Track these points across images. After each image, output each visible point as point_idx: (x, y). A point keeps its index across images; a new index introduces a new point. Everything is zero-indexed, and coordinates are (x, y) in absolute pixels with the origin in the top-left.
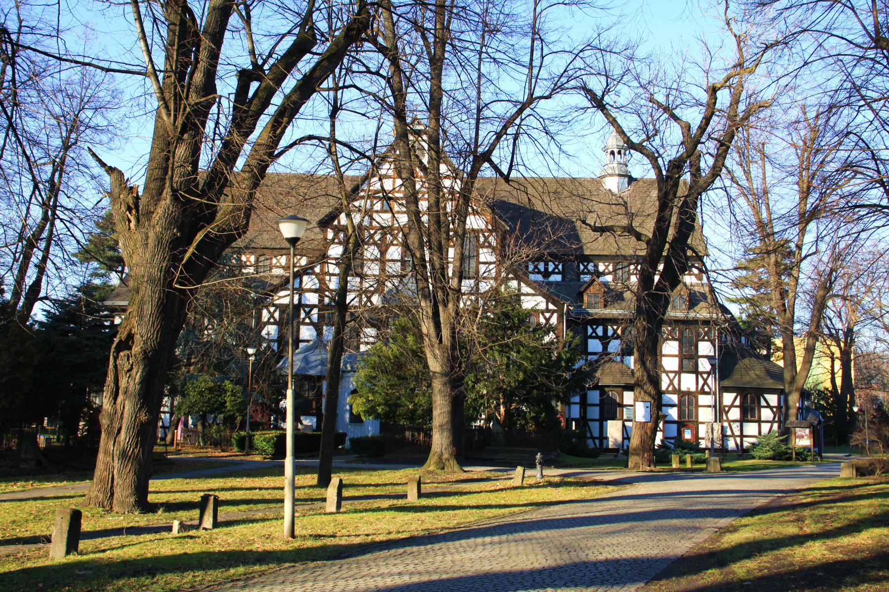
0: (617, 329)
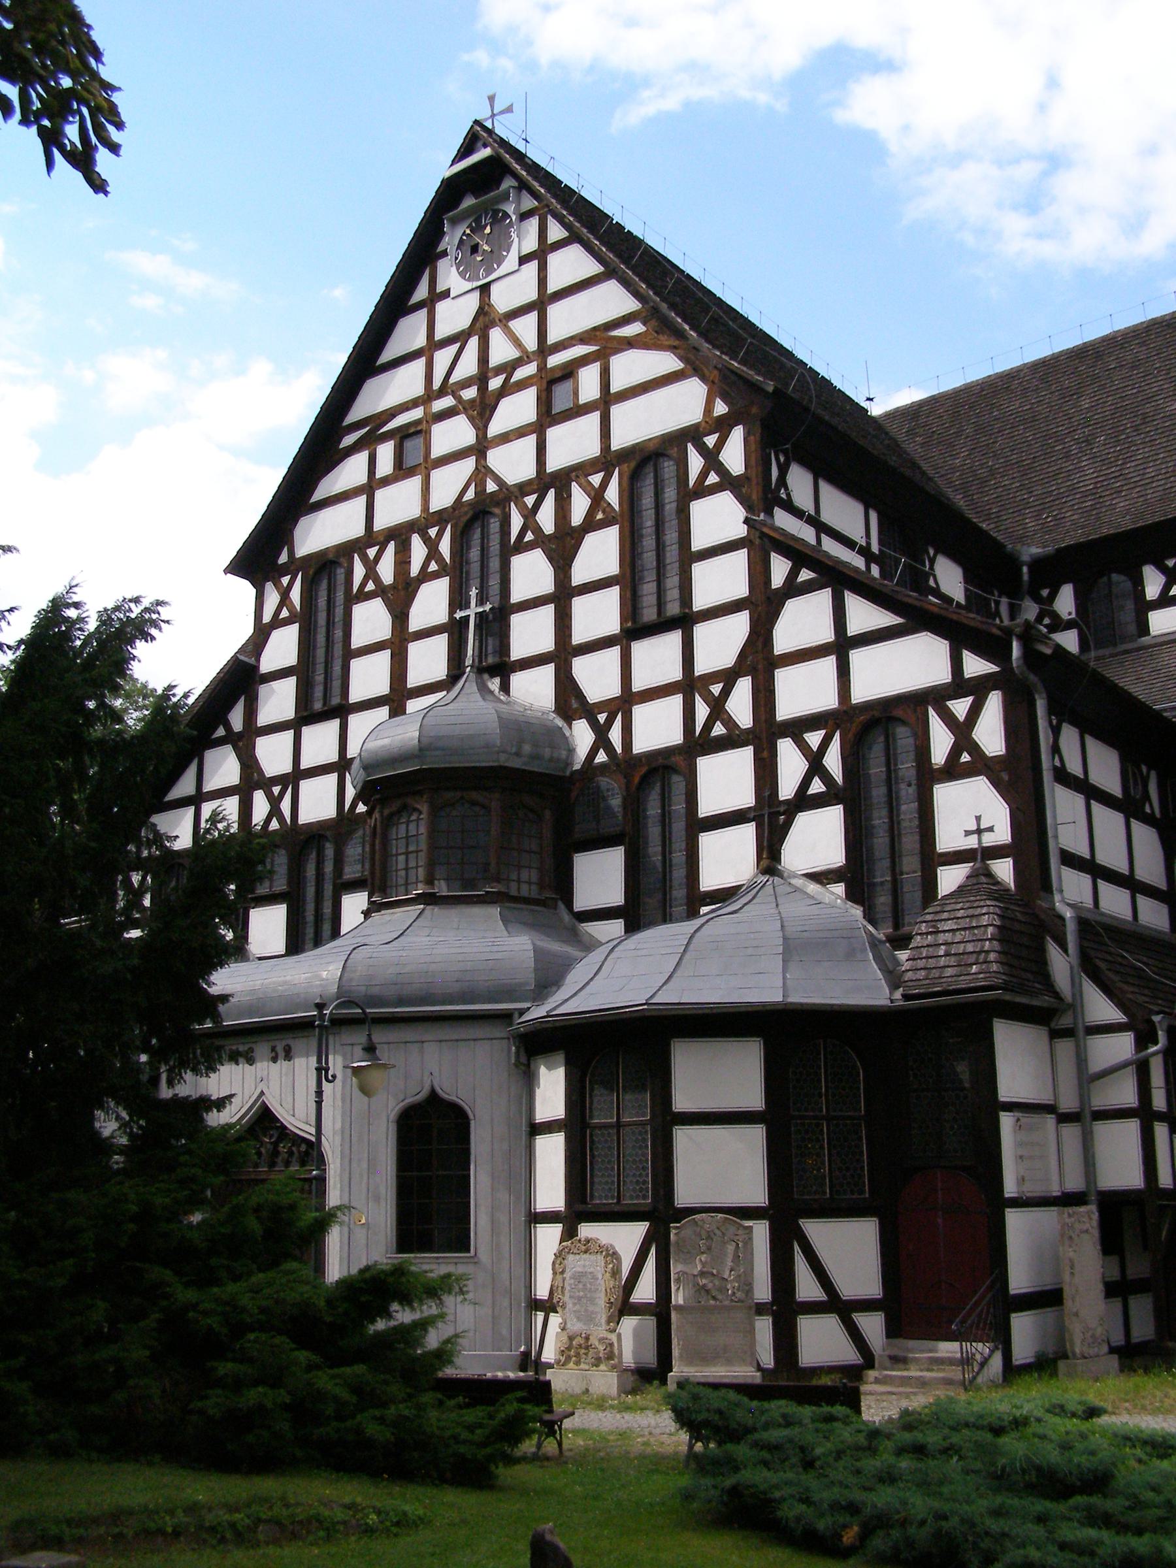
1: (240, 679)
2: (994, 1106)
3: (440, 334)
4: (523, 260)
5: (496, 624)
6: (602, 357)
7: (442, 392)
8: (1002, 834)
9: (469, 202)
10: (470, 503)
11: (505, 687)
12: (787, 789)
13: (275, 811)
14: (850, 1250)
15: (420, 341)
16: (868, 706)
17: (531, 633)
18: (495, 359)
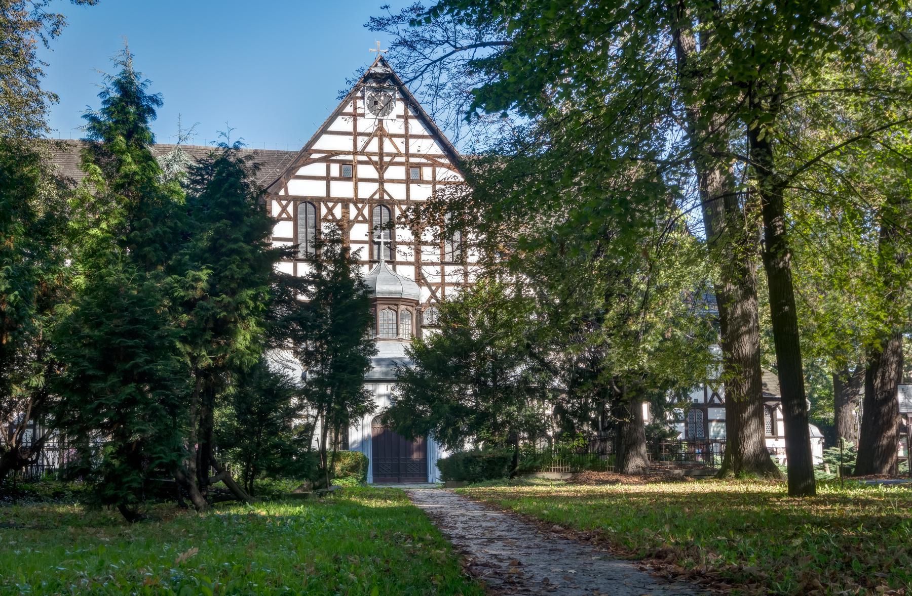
7: (362, 153)
10: (376, 200)
11: (394, 269)
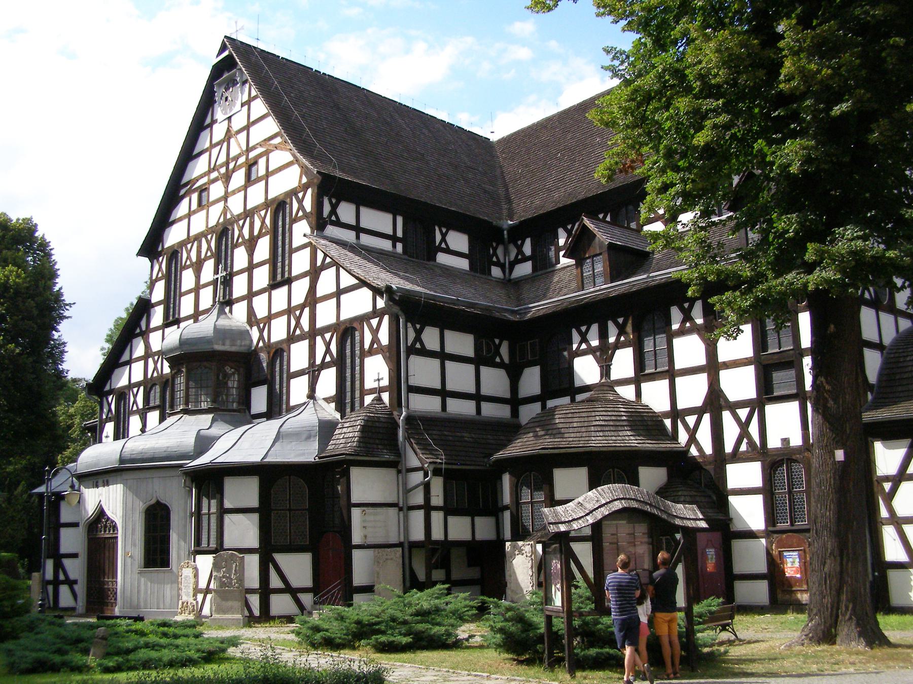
0: (625, 322)
1: (143, 307)
2: (350, 505)
3: (214, 142)
4: (243, 105)
5: (227, 282)
6: (266, 153)
7: (214, 170)
8: (385, 382)
9: (226, 75)
11: (231, 311)
12: (318, 361)
13: (155, 368)
14: (297, 567)
15: (207, 145)
16: (345, 321)
17: (240, 286)
18: (232, 155)
